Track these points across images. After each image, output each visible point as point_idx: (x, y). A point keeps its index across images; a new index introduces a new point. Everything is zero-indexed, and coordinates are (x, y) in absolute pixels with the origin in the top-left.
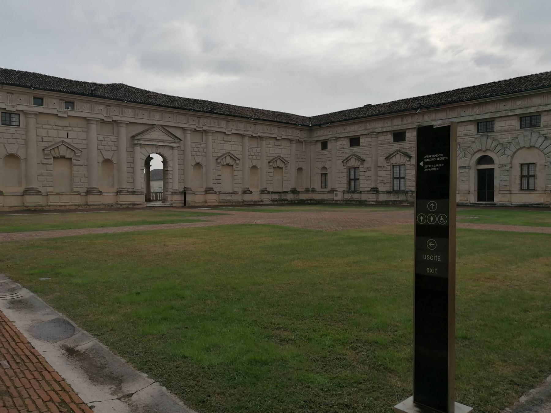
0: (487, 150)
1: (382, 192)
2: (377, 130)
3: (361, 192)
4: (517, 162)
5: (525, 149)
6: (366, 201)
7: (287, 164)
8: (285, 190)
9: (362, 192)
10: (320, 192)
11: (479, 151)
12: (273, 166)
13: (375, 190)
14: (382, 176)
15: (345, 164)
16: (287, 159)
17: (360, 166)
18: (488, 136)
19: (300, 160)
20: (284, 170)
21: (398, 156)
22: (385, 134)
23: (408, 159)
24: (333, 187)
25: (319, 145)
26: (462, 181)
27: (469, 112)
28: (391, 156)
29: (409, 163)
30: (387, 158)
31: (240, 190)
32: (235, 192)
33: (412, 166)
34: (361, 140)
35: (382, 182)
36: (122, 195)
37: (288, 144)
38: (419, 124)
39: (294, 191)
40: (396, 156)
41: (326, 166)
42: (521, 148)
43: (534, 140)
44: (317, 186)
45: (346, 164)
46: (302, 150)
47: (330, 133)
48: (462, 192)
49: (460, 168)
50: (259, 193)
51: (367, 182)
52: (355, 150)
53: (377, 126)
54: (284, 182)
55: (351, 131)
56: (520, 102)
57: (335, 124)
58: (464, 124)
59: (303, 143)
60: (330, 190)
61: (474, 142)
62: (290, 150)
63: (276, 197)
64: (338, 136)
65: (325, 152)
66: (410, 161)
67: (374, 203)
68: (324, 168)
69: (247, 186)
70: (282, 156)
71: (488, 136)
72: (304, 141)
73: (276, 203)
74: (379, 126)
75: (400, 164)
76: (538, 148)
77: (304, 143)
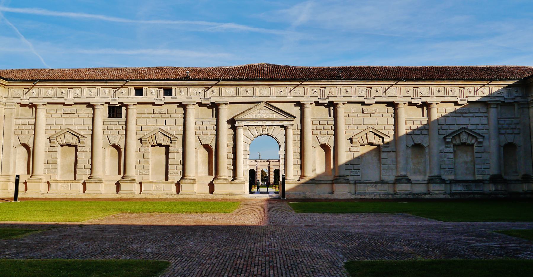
12: (454, 142)
19: (510, 131)
20: (476, 149)
31: (392, 178)
32: (383, 180)
36: (218, 183)
37: (483, 110)
50: (426, 182)
62: (486, 118)
63: (459, 188)
69: (403, 173)
70: (470, 127)
77: (516, 105)
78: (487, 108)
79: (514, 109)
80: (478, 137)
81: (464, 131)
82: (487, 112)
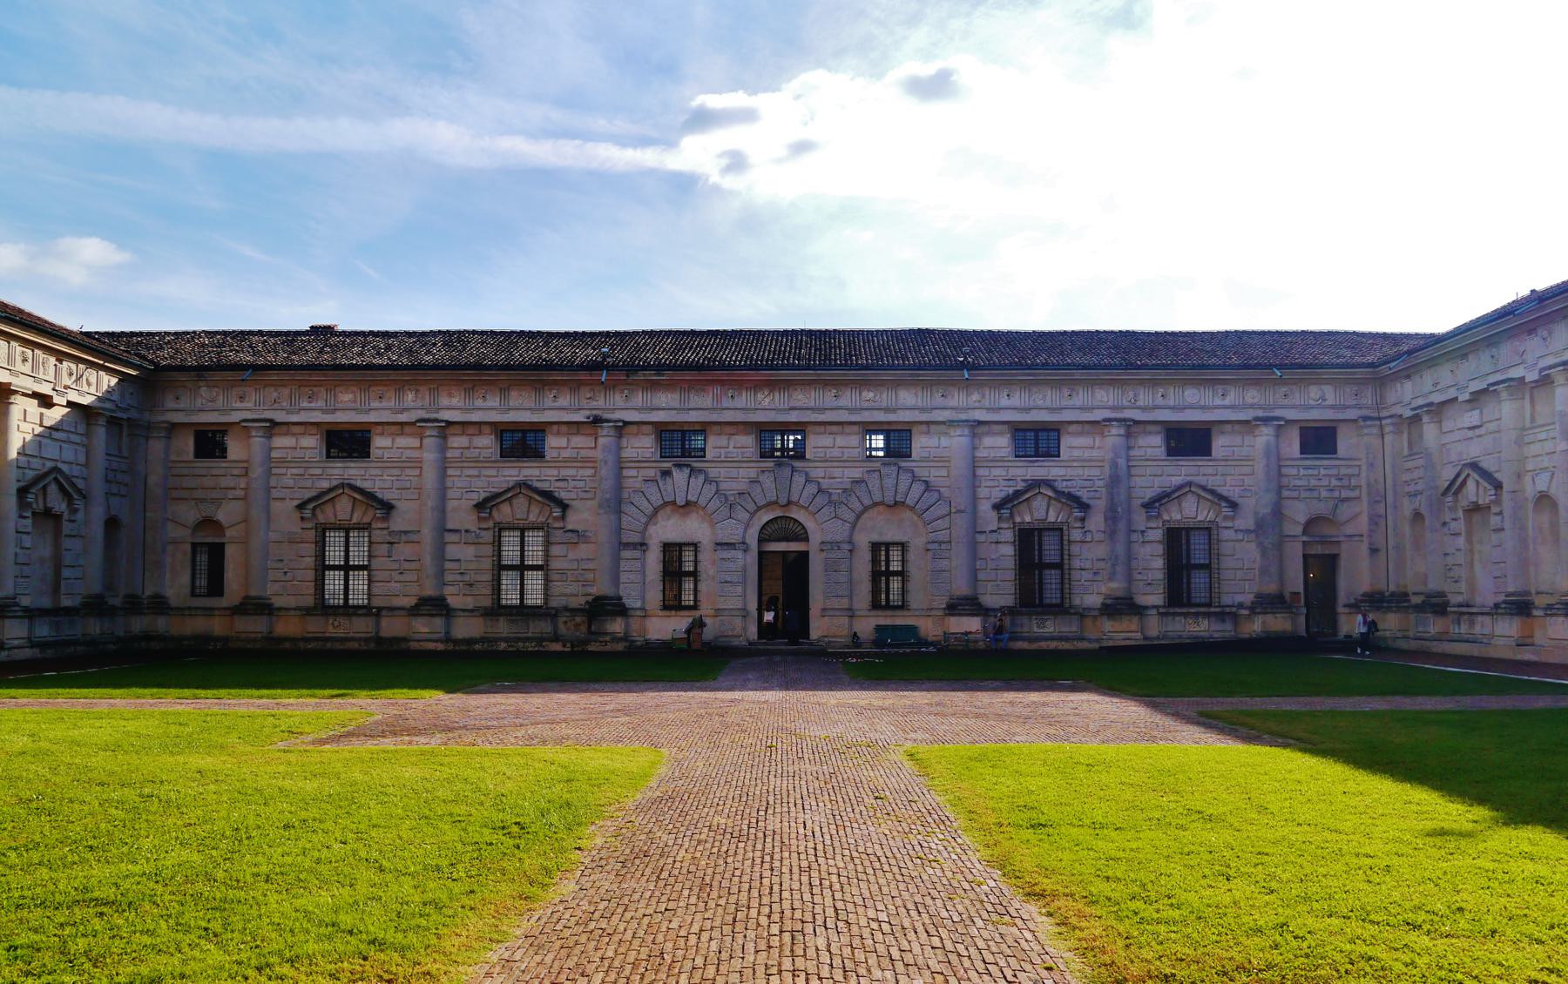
0: (789, 503)
1: (464, 610)
2: (447, 415)
3: (380, 609)
4: (863, 540)
5: (881, 508)
6: (405, 640)
7: (79, 504)
8: (66, 602)
9: (384, 613)
10: (190, 608)
11: (770, 504)
13: (434, 606)
14: (459, 560)
15: (307, 513)
16: (80, 484)
17: (374, 526)
18: (793, 470)
21: (520, 503)
22: (471, 430)
23: (557, 512)
24: (253, 593)
25: (188, 444)
26: (726, 582)
27: (744, 399)
28: (498, 500)
29: (561, 525)
30: (480, 506)
33: (570, 534)
34: (379, 442)
35: (459, 578)
38: (595, 412)
39: (95, 606)
40: (515, 501)
41: (221, 516)
42: (876, 504)
43: (902, 487)
44: (176, 584)
45: (314, 514)
46: (117, 453)
47: (249, 405)
48: (727, 613)
49: (719, 548)
51: (402, 578)
52: (352, 471)
53: (444, 401)
54: (66, 573)
55: (340, 406)
56: (871, 395)
57: (274, 376)
58: (728, 429)
59: (120, 426)
60: (241, 604)
61: (754, 481)
63: (43, 630)
64: (280, 417)
65: (216, 465)
66: (563, 518)
67: (441, 647)
68: (209, 523)
70: (65, 468)
71: (793, 470)
72: (129, 419)
73: (50, 653)
74: (453, 405)
75: (526, 526)
76: (912, 509)
78: (88, 424)
79: (120, 437)
80: (76, 497)
81: (56, 479)
82: (87, 435)
